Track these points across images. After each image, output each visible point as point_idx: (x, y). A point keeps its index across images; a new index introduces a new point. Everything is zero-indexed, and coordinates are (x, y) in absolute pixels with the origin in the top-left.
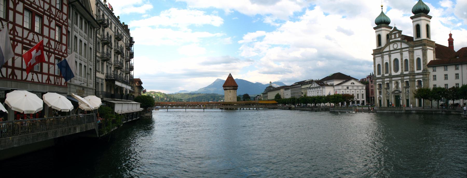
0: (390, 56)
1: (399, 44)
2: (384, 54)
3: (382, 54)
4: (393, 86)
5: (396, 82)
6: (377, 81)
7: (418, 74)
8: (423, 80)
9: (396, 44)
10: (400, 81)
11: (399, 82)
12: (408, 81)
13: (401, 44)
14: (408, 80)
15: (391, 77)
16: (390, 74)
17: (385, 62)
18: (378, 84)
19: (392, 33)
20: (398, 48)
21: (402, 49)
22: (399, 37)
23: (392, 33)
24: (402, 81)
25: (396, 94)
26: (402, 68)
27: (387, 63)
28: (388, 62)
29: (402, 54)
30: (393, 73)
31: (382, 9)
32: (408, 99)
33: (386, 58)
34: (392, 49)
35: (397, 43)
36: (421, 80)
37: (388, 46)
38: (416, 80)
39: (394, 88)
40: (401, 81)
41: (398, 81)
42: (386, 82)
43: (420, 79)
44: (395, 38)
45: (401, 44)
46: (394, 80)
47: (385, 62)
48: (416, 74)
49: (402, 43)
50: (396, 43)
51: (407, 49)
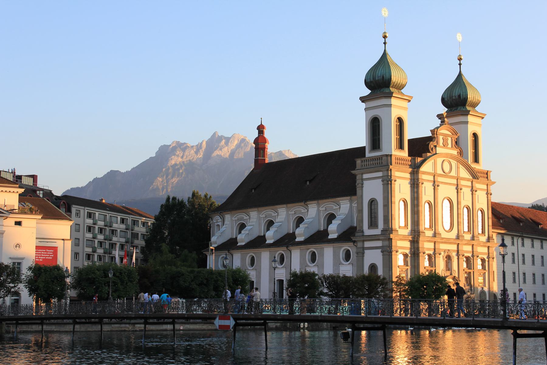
5: (446, 254)
10: (454, 254)
11: (453, 256)
12: (469, 257)
13: (458, 168)
19: (451, 134)
31: (385, 43)
34: (440, 171)
35: (451, 162)
36: (485, 257)
39: (443, 270)
40: (458, 255)
41: (450, 254)
42: (427, 252)
44: (445, 145)
45: (458, 168)
49: (461, 166)
50: (451, 160)
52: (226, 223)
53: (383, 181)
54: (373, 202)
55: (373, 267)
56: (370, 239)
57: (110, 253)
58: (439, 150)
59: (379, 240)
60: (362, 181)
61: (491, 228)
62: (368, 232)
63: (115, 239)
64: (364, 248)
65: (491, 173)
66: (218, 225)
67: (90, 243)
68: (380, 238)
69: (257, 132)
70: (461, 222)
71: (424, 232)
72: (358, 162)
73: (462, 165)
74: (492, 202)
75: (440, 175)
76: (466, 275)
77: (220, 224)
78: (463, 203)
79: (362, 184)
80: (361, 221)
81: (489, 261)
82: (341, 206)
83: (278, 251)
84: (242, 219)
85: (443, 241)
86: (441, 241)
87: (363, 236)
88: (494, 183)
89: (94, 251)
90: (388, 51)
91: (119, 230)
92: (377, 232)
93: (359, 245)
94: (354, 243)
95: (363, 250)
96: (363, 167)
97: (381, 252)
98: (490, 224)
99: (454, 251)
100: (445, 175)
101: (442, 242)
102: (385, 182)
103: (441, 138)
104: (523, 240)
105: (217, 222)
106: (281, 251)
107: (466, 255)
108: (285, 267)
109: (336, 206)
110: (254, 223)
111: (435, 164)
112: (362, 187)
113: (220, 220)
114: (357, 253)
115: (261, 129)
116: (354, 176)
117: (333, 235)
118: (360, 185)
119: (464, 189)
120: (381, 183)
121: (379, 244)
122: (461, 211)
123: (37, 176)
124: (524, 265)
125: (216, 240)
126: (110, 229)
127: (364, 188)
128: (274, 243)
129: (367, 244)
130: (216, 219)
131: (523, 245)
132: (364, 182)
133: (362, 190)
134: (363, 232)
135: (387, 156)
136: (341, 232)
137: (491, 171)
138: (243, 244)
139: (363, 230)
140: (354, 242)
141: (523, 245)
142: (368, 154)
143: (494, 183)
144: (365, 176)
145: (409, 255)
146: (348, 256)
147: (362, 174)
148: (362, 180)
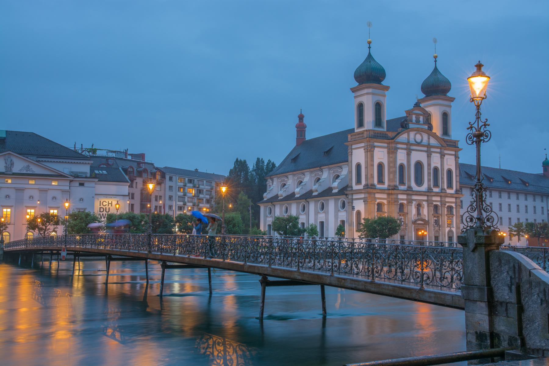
0: (409, 155)
1: (425, 137)
2: (399, 146)
3: (393, 145)
4: (414, 211)
5: (417, 203)
6: (377, 196)
7: (451, 196)
8: (456, 206)
9: (421, 134)
10: (425, 204)
14: (439, 203)
15: (409, 191)
16: (410, 188)
17: (399, 163)
18: (378, 203)
19: (422, 113)
20: (422, 144)
21: (429, 146)
22: (424, 124)
23: (414, 112)
24: (429, 202)
25: (419, 226)
26: (429, 180)
27: (402, 167)
28: (405, 163)
29: (429, 156)
30: (415, 187)
31: (369, 48)
32: (437, 235)
33: (401, 157)
34: (412, 140)
35: (423, 135)
36: (453, 205)
37: (406, 134)
38: (447, 204)
41: (421, 203)
43: (451, 204)
45: (429, 139)
46: (415, 200)
47: (399, 163)
48: (450, 196)
51: (438, 150)
52: (274, 183)
53: (364, 149)
54: (358, 166)
55: (359, 213)
56: (356, 192)
57: (198, 206)
58: (411, 126)
59: (362, 193)
60: (352, 150)
61: (458, 184)
62: (355, 187)
63: (201, 196)
64: (352, 199)
65: (459, 143)
66: (270, 185)
67: (181, 199)
68: (363, 191)
69: (298, 118)
70: (430, 179)
71: (398, 187)
72: (349, 136)
73: (432, 136)
74: (460, 164)
75: (412, 145)
76: (436, 219)
77: (271, 184)
78: (433, 166)
79: (352, 153)
80: (351, 179)
81: (456, 208)
82: (343, 169)
83: (301, 202)
84: (284, 181)
85: (414, 193)
86: (412, 193)
87: (352, 190)
88: (461, 149)
89: (185, 204)
90: (373, 54)
91: (205, 190)
92: (361, 187)
93: (350, 197)
94: (346, 196)
95: (352, 201)
96: (352, 140)
97: (364, 201)
98: (458, 180)
99: (424, 200)
100: (418, 144)
101: (413, 194)
102: (366, 150)
103: (414, 117)
104: (491, 192)
105: (269, 183)
106: (303, 202)
107: (434, 203)
108: (305, 214)
109: (340, 169)
110: (290, 183)
111: (409, 136)
112: (352, 155)
113: (271, 182)
114: (349, 203)
115: (301, 117)
116: (347, 146)
117: (335, 190)
118: (350, 153)
119: (433, 154)
120: (364, 151)
121: (362, 196)
122: (430, 171)
123: (144, 154)
124: (501, 212)
125: (267, 196)
126: (197, 190)
127: (353, 155)
128: (300, 196)
129: (355, 197)
130: (269, 182)
131: (491, 196)
132: (353, 151)
133: (352, 156)
134: (352, 187)
135: (367, 131)
136: (341, 188)
137: (459, 141)
138: (282, 198)
139: (352, 186)
140: (346, 195)
141: (491, 196)
142: (356, 131)
143: (461, 149)
144: (354, 147)
145: (386, 204)
146: (343, 206)
147: (352, 145)
148: (352, 149)
